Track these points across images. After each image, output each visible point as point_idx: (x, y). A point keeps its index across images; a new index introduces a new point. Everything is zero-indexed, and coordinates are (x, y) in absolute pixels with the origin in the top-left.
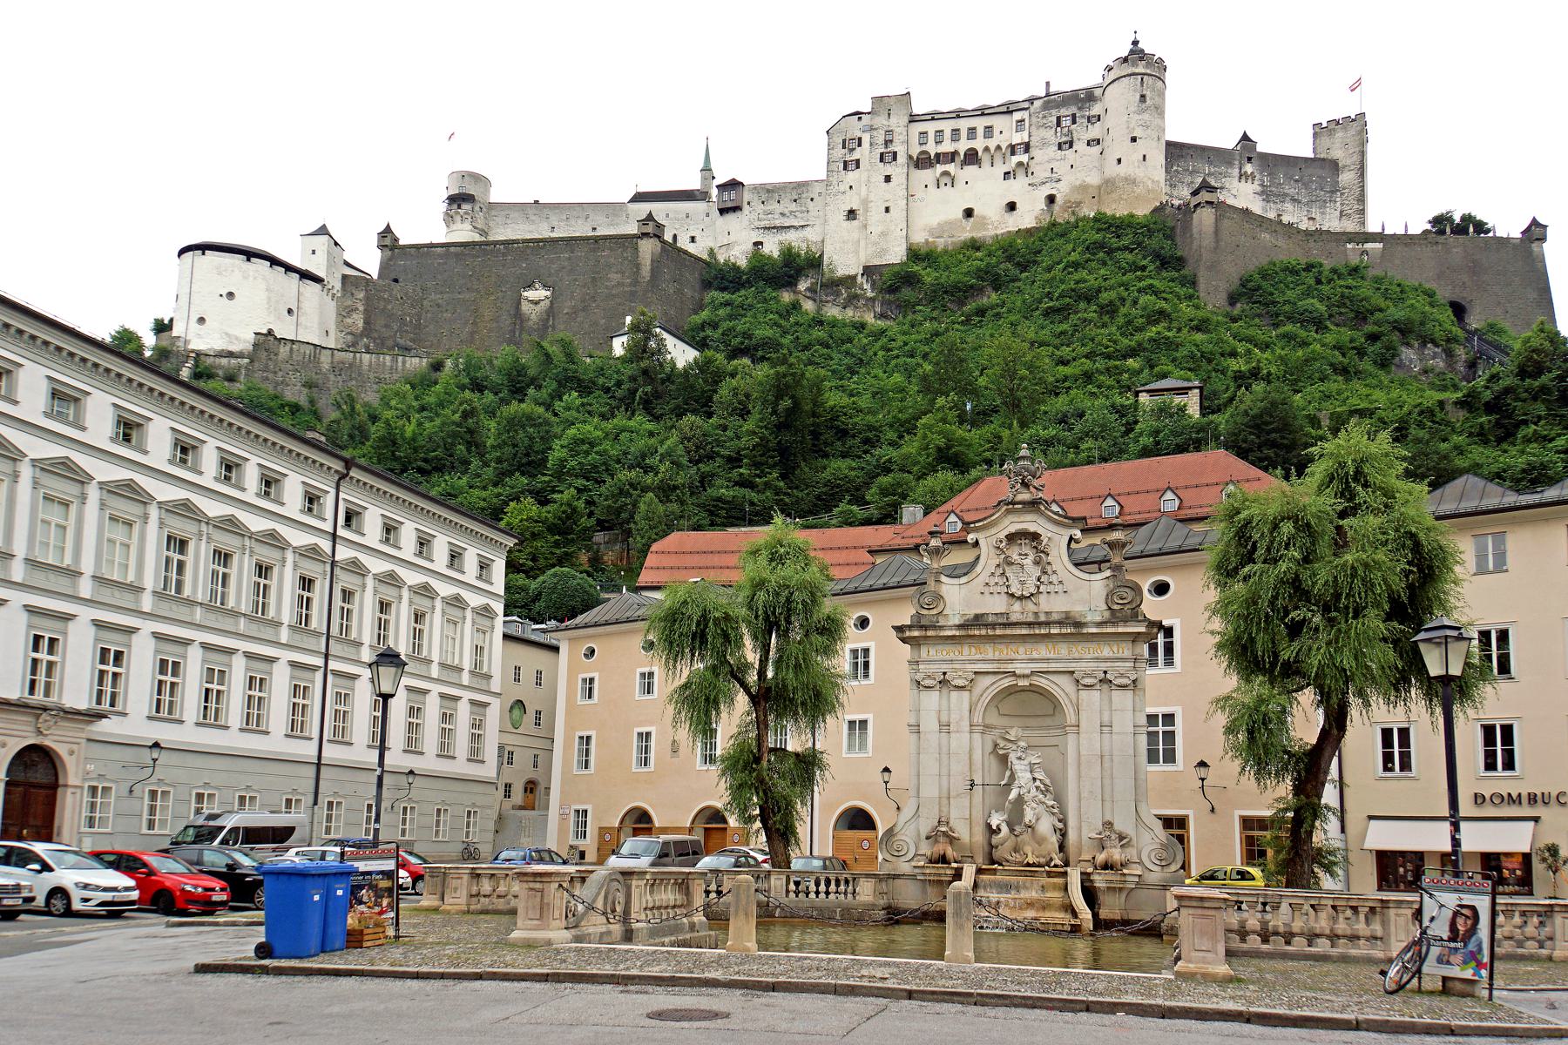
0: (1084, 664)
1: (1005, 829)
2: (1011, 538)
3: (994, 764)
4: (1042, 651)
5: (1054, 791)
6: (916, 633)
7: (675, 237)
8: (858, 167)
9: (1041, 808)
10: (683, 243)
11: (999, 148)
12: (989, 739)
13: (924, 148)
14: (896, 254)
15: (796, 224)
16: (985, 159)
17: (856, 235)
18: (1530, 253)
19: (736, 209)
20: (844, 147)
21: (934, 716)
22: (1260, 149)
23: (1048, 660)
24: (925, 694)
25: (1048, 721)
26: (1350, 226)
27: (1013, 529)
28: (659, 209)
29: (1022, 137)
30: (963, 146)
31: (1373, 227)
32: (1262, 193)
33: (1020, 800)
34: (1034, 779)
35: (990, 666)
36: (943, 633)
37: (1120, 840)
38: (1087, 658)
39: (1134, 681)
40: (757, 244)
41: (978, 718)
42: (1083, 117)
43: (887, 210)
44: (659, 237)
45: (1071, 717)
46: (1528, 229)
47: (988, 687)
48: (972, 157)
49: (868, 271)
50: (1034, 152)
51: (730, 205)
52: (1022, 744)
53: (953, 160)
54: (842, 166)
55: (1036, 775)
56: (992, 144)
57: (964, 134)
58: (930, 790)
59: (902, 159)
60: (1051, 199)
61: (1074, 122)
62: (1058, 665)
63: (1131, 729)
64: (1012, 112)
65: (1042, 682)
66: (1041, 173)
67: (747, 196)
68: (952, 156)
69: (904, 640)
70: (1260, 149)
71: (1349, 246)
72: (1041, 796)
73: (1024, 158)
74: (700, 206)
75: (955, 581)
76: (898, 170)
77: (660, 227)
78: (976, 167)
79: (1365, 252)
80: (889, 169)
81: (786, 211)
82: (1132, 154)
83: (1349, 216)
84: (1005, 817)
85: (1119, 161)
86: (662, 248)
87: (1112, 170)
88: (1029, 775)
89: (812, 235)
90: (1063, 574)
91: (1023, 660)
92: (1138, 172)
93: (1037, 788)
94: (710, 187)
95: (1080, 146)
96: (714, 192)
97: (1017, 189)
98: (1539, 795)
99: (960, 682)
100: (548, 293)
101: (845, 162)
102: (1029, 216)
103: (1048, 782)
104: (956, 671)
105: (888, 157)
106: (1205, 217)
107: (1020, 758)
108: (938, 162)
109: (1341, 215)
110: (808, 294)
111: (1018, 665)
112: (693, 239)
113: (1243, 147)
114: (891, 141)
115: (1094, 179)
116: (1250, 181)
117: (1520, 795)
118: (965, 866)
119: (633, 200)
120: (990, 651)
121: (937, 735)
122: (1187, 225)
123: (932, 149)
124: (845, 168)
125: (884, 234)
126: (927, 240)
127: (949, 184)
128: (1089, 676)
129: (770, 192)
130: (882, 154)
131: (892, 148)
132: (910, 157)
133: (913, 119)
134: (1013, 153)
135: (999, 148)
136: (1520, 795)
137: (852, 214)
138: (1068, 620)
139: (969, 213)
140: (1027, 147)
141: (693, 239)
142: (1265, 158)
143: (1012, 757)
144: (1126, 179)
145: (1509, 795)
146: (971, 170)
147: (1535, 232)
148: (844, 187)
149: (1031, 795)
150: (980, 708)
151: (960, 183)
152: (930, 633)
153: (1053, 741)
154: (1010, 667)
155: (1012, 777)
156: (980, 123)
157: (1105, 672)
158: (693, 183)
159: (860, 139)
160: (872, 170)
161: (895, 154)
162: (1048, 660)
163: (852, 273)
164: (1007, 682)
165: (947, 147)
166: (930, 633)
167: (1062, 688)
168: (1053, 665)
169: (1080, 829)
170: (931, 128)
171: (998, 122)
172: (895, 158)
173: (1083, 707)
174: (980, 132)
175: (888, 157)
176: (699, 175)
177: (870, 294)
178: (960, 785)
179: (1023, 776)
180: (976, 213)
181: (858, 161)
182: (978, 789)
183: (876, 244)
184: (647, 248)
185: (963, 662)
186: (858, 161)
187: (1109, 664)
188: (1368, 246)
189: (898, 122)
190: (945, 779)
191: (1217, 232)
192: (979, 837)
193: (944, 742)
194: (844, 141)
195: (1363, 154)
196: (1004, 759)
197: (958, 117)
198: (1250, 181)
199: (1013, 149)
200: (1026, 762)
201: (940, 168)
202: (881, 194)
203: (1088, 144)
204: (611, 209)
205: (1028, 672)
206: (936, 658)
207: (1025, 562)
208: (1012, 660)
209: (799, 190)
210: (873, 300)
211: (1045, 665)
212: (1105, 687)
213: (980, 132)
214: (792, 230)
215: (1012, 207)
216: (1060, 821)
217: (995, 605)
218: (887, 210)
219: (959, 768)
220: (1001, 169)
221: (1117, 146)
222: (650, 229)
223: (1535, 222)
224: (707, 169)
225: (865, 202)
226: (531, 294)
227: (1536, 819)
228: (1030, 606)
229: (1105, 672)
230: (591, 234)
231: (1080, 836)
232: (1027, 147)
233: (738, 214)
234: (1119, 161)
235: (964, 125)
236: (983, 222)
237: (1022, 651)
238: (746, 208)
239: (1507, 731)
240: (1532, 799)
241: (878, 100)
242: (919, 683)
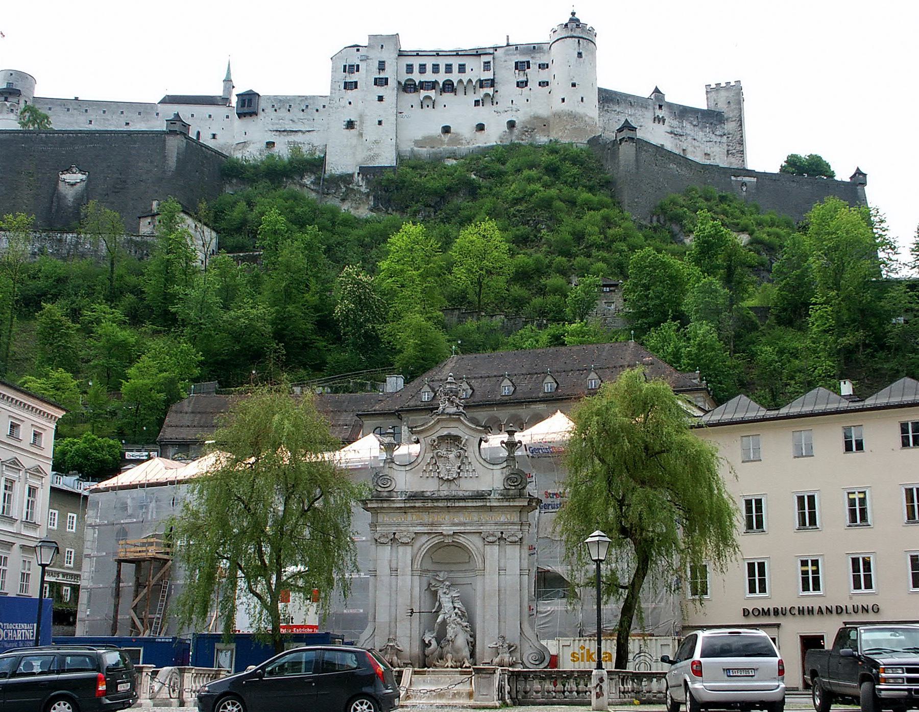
1: (434, 643)
2: (442, 438)
3: (427, 598)
4: (461, 518)
5: (468, 616)
6: (375, 505)
7: (199, 133)
8: (356, 87)
10: (206, 140)
11: (470, 81)
12: (425, 580)
13: (410, 76)
14: (387, 159)
15: (303, 129)
16: (460, 91)
17: (354, 141)
18: (856, 192)
19: (254, 114)
20: (345, 71)
21: (386, 563)
22: (667, 99)
23: (464, 524)
24: (380, 548)
25: (466, 567)
26: (734, 163)
27: (445, 432)
28: (184, 111)
29: (488, 75)
30: (441, 77)
31: (751, 165)
32: (671, 133)
33: (444, 623)
34: (455, 608)
35: (426, 528)
36: (393, 505)
38: (491, 523)
39: (521, 539)
40: (270, 144)
42: (535, 64)
43: (380, 123)
44: (185, 135)
45: (479, 565)
46: (855, 174)
47: (424, 543)
48: (448, 87)
49: (364, 171)
50: (497, 87)
51: (246, 110)
52: (447, 583)
53: (433, 88)
54: (342, 86)
55: (456, 605)
56: (465, 78)
57: (442, 69)
58: (383, 617)
59: (392, 83)
60: (511, 124)
61: (529, 68)
63: (518, 572)
64: (480, 55)
65: (461, 540)
66: (503, 104)
67: (262, 104)
68: (433, 85)
69: (367, 509)
70: (667, 99)
71: (733, 178)
72: (459, 619)
73: (490, 91)
74: (221, 111)
75: (403, 468)
76: (389, 92)
77: (186, 126)
78: (453, 94)
79: (744, 184)
80: (381, 90)
81: (295, 119)
82: (573, 97)
83: (733, 154)
84: (434, 635)
85: (563, 100)
86: (187, 143)
87: (558, 106)
88: (451, 605)
89: (316, 140)
91: (447, 525)
92: (580, 109)
93: (456, 614)
94: (230, 94)
95: (533, 84)
96: (234, 100)
97: (484, 114)
98: (780, 609)
99: (405, 540)
100: (84, 177)
101: (346, 83)
102: (494, 136)
103: (463, 609)
104: (402, 531)
105: (381, 82)
106: (627, 151)
107: (445, 593)
108: (422, 88)
109: (728, 154)
110: (312, 187)
111: (445, 528)
112: (214, 136)
113: (655, 96)
114: (383, 70)
115: (544, 112)
116: (661, 123)
117: (769, 609)
118: (405, 670)
119: (164, 101)
120: (427, 518)
121: (388, 578)
122: (615, 154)
123: (417, 77)
124: (345, 88)
125: (376, 142)
126: (412, 151)
127: (431, 106)
128: (493, 535)
129: (283, 103)
130: (376, 79)
131: (382, 76)
132: (399, 83)
133: (401, 54)
134: (481, 87)
135: (470, 81)
136: (769, 609)
137: (350, 125)
138: (480, 496)
139: (446, 130)
140: (492, 83)
141: (214, 136)
142: (671, 106)
143: (440, 592)
144: (569, 115)
145: (763, 609)
146: (448, 96)
147: (859, 178)
148: (344, 102)
149: (452, 619)
150: (419, 559)
151: (439, 107)
152: (385, 505)
153: (468, 581)
154: (439, 530)
155: (440, 606)
156: (455, 62)
157: (502, 533)
158: (217, 90)
159: (358, 66)
160: (367, 91)
161: (387, 79)
162: (464, 524)
163: (350, 172)
164: (436, 540)
165: (429, 76)
166: (385, 505)
167: (473, 543)
168: (468, 528)
169: (483, 640)
170: (416, 62)
171: (469, 63)
172: (386, 84)
173: (488, 557)
174: (455, 68)
175: (381, 82)
176: (222, 84)
177: (364, 189)
178: (403, 612)
179: (447, 605)
180: (452, 131)
181: (356, 83)
182: (415, 615)
183: (370, 149)
184: (174, 144)
185: (407, 526)
186: (356, 83)
187: (504, 527)
188: (747, 179)
189: (389, 56)
190: (393, 609)
191: (637, 160)
192: (417, 650)
193: (394, 583)
194: (345, 66)
195: (740, 110)
196: (435, 594)
197: (438, 55)
198: (661, 123)
199: (481, 83)
201: (423, 93)
202: (375, 111)
203: (540, 85)
204: (142, 109)
205: (451, 533)
206: (390, 522)
207: (450, 456)
208: (441, 524)
209: (306, 104)
210: (368, 195)
211: (463, 528)
212: (502, 542)
213: (455, 68)
214: (300, 134)
215: (481, 127)
216: (471, 636)
217: (430, 486)
218: (380, 123)
219: (403, 601)
220: (472, 97)
221: (559, 88)
222: (177, 127)
223: (858, 172)
224: (228, 82)
225: (361, 116)
226: (68, 177)
227: (778, 626)
228: (453, 487)
229: (502, 533)
230: (126, 128)
231: (484, 648)
232: (492, 83)
233: (254, 117)
234: (563, 100)
235: (442, 62)
236: (457, 140)
237: (446, 517)
238: (261, 115)
239: (762, 566)
240: (776, 612)
241: (371, 37)
242: (376, 540)
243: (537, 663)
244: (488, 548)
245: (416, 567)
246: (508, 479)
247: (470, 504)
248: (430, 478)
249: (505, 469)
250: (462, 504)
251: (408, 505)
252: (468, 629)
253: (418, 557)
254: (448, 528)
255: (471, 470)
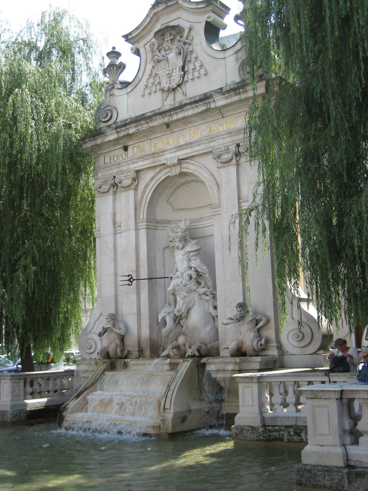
0: (221, 141)
9: (195, 296)
37: (257, 324)
41: (143, 214)
62: (202, 147)
65: (190, 167)
90: (203, 58)
103: (203, 269)
104: (122, 172)
111: (168, 156)
154: (163, 159)
164: (162, 176)
168: (196, 148)
200: (182, 252)
205: (176, 161)
211: (189, 151)
243: (302, 344)
244: (223, 171)
245: (141, 217)
246: (242, 67)
247: (190, 113)
248: (153, 94)
249: (240, 54)
250: (181, 115)
251: (121, 134)
252: (207, 298)
253: (143, 202)
254: (172, 155)
255: (198, 68)
